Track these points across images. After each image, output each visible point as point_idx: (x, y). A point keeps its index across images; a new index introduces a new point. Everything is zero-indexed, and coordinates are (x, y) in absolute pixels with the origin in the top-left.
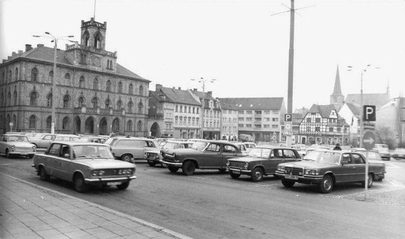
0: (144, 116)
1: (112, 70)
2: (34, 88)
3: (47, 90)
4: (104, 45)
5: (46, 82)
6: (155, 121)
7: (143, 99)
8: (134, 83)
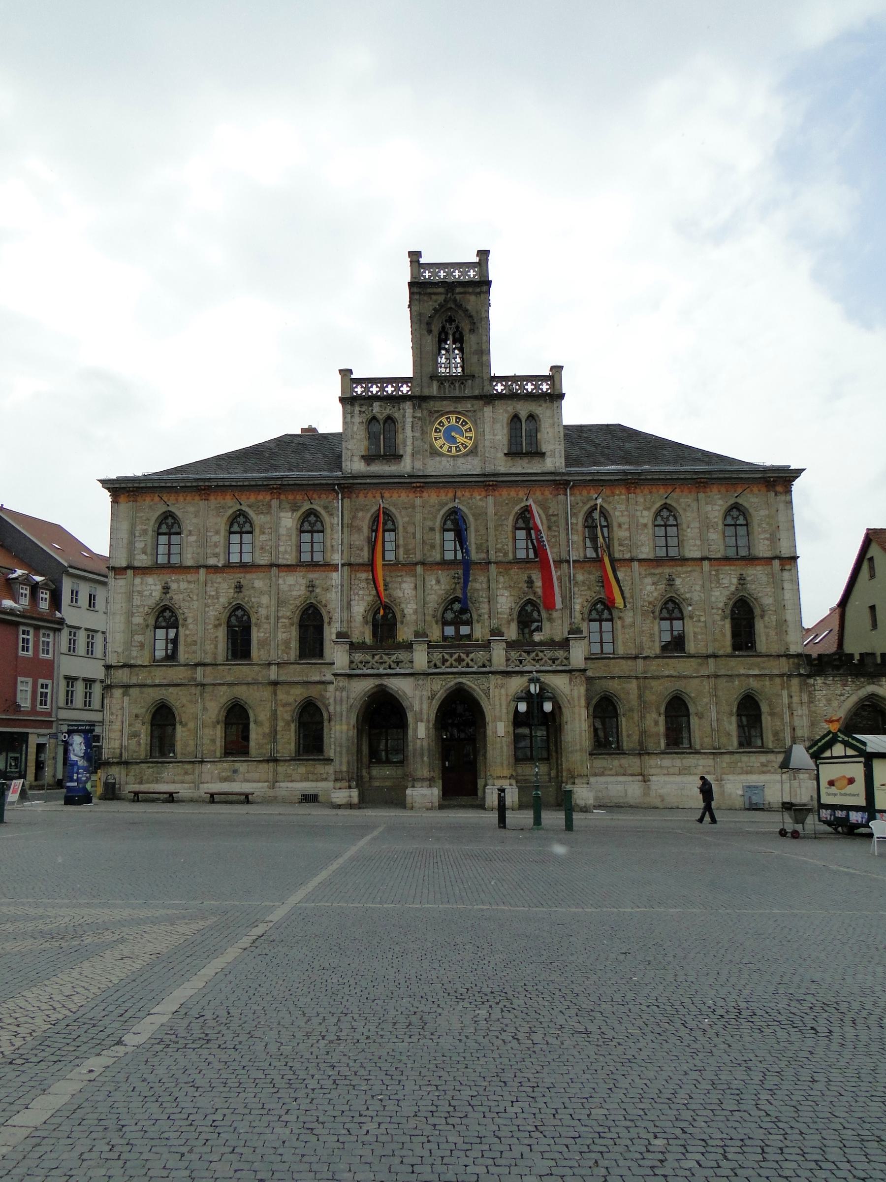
0: (784, 666)
1: (542, 455)
2: (166, 589)
3: (223, 590)
4: (484, 352)
5: (212, 561)
6: (871, 689)
7: (757, 575)
8: (685, 502)
